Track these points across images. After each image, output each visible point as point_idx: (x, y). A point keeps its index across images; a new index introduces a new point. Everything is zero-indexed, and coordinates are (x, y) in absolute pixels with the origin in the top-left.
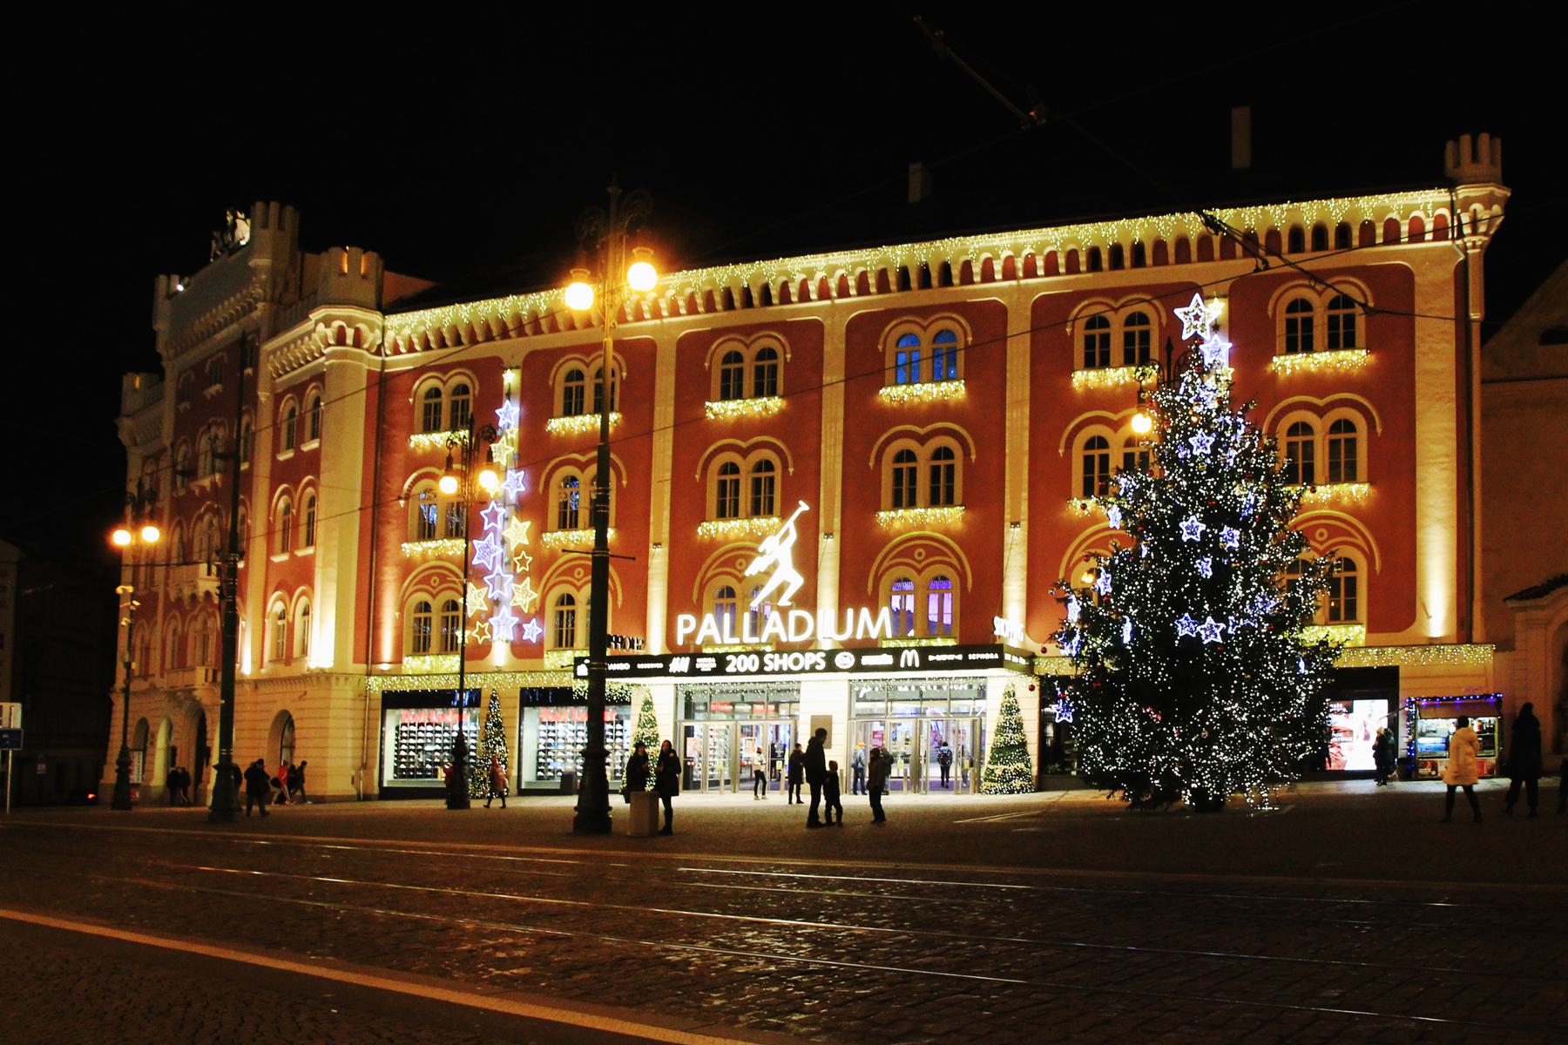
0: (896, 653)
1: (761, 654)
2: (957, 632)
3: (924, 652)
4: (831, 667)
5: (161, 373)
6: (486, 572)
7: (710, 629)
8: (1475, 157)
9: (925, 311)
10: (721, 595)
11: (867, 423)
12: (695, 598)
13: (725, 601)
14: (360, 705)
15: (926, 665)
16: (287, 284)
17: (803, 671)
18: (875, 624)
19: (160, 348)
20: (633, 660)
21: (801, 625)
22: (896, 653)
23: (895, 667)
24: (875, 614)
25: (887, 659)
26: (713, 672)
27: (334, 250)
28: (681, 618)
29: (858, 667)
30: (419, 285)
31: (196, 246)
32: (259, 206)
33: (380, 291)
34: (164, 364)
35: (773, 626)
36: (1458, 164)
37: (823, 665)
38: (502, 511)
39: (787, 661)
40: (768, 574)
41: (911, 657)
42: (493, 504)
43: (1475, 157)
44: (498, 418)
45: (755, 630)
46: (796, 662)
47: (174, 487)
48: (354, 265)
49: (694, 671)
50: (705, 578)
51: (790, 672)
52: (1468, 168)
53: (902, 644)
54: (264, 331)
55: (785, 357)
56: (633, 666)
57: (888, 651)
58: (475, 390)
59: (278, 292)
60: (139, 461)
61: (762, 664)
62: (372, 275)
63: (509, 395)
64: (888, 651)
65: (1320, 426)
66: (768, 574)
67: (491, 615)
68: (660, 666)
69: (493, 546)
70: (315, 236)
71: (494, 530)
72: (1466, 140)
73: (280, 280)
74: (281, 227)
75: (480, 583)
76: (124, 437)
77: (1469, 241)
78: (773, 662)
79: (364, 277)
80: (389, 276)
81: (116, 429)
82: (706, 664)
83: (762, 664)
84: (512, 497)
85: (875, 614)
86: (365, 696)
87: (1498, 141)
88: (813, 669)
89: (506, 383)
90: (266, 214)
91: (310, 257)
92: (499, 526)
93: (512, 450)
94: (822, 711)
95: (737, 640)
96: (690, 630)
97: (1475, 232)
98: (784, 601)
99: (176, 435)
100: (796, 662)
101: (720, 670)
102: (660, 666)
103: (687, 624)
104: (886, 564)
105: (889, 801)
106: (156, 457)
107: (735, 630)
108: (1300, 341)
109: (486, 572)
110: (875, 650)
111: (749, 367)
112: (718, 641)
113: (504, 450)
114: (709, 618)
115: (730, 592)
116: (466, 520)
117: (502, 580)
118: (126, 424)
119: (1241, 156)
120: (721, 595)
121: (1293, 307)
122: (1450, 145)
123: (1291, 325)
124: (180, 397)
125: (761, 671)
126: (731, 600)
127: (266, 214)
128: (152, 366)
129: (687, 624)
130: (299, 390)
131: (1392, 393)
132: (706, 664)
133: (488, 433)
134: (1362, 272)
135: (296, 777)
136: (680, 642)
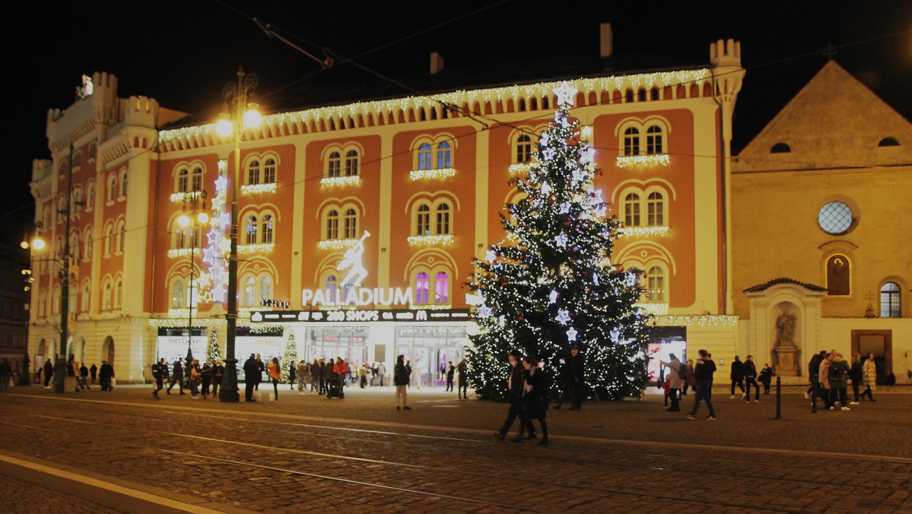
0: (415, 312)
1: (345, 311)
2: (450, 300)
3: (429, 312)
4: (381, 319)
5: (51, 159)
6: (209, 265)
7: (321, 297)
8: (726, 52)
9: (434, 132)
10: (329, 280)
11: (403, 191)
12: (315, 280)
13: (331, 282)
14: (147, 334)
15: (430, 319)
16: (111, 115)
17: (367, 321)
18: (404, 296)
19: (50, 147)
20: (281, 313)
21: (366, 296)
22: (415, 312)
23: (414, 320)
24: (404, 292)
25: (410, 315)
26: (321, 320)
27: (133, 98)
28: (305, 291)
29: (395, 320)
30: (180, 115)
31: (68, 96)
32: (97, 74)
33: (156, 120)
34: (52, 155)
35: (352, 296)
36: (716, 56)
37: (377, 317)
38: (218, 234)
39: (358, 315)
40: (350, 268)
41: (422, 315)
42: (213, 230)
43: (726, 52)
44: (215, 185)
45: (344, 297)
46: (363, 316)
47: (57, 220)
48: (143, 106)
49: (311, 320)
50: (316, 269)
51: (360, 321)
52: (722, 59)
53: (418, 308)
54: (99, 140)
55: (278, 161)
56: (281, 317)
57: (411, 311)
58: (205, 171)
59: (107, 118)
60: (41, 206)
61: (346, 317)
62: (152, 111)
63: (221, 174)
64: (411, 311)
65: (643, 196)
66: (350, 268)
67: (212, 288)
68: (294, 316)
69: (213, 252)
70: (125, 91)
71: (214, 244)
72: (721, 43)
73: (108, 113)
74: (108, 84)
75: (207, 271)
76: (33, 193)
77: (723, 96)
78: (351, 315)
79: (148, 112)
80: (161, 109)
81: (29, 188)
82: (317, 316)
83: (346, 317)
84: (223, 227)
85: (404, 292)
86: (149, 329)
87: (738, 44)
88: (372, 320)
89: (220, 167)
90: (100, 79)
91: (122, 100)
92: (216, 242)
93: (224, 202)
94: (380, 343)
95: (333, 304)
96: (309, 298)
97: (726, 92)
98: (357, 283)
99: (59, 191)
100: (363, 316)
101: (324, 319)
102: (294, 316)
103: (308, 294)
104: (414, 265)
105: (410, 390)
106: (49, 203)
107: (333, 299)
108: (632, 148)
109: (209, 265)
110: (406, 310)
111: (262, 168)
112: (324, 304)
113: (219, 202)
114: (319, 291)
115: (334, 278)
116: (199, 239)
117: (218, 270)
118: (34, 186)
119: (606, 49)
120: (329, 280)
121: (628, 132)
122: (712, 46)
123: (627, 141)
124: (61, 172)
125: (345, 320)
126: (334, 282)
127: (100, 79)
128: (46, 155)
129: (308, 294)
130: (117, 169)
131: (682, 175)
132: (317, 316)
133: (210, 192)
134: (666, 114)
135: (108, 370)
136: (304, 304)
